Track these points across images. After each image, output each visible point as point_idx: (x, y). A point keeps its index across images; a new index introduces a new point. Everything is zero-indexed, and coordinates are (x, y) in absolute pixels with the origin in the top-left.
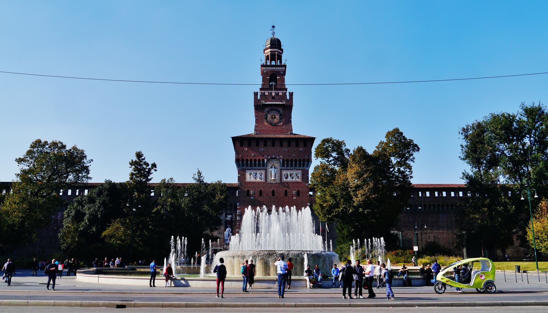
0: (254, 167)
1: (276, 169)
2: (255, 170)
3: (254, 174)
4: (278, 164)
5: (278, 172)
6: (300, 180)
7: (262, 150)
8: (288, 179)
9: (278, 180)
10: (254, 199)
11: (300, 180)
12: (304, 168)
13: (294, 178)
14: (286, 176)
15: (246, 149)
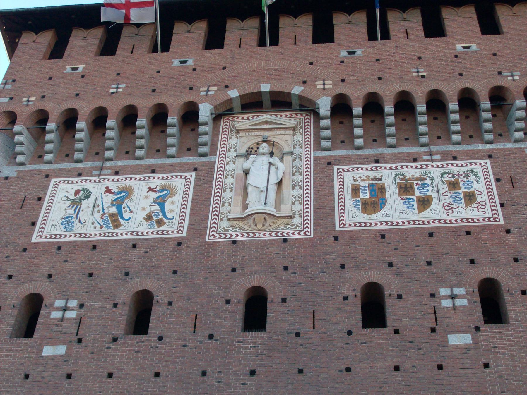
0: (117, 157)
1: (288, 159)
2: (117, 173)
3: (109, 198)
4: (298, 137)
5: (298, 178)
6: (489, 214)
7: (190, 62)
8: (385, 209)
9: (297, 220)
10: (65, 358)
11: (489, 214)
12: (509, 145)
13: (435, 204)
14: (365, 195)
15: (81, 67)
